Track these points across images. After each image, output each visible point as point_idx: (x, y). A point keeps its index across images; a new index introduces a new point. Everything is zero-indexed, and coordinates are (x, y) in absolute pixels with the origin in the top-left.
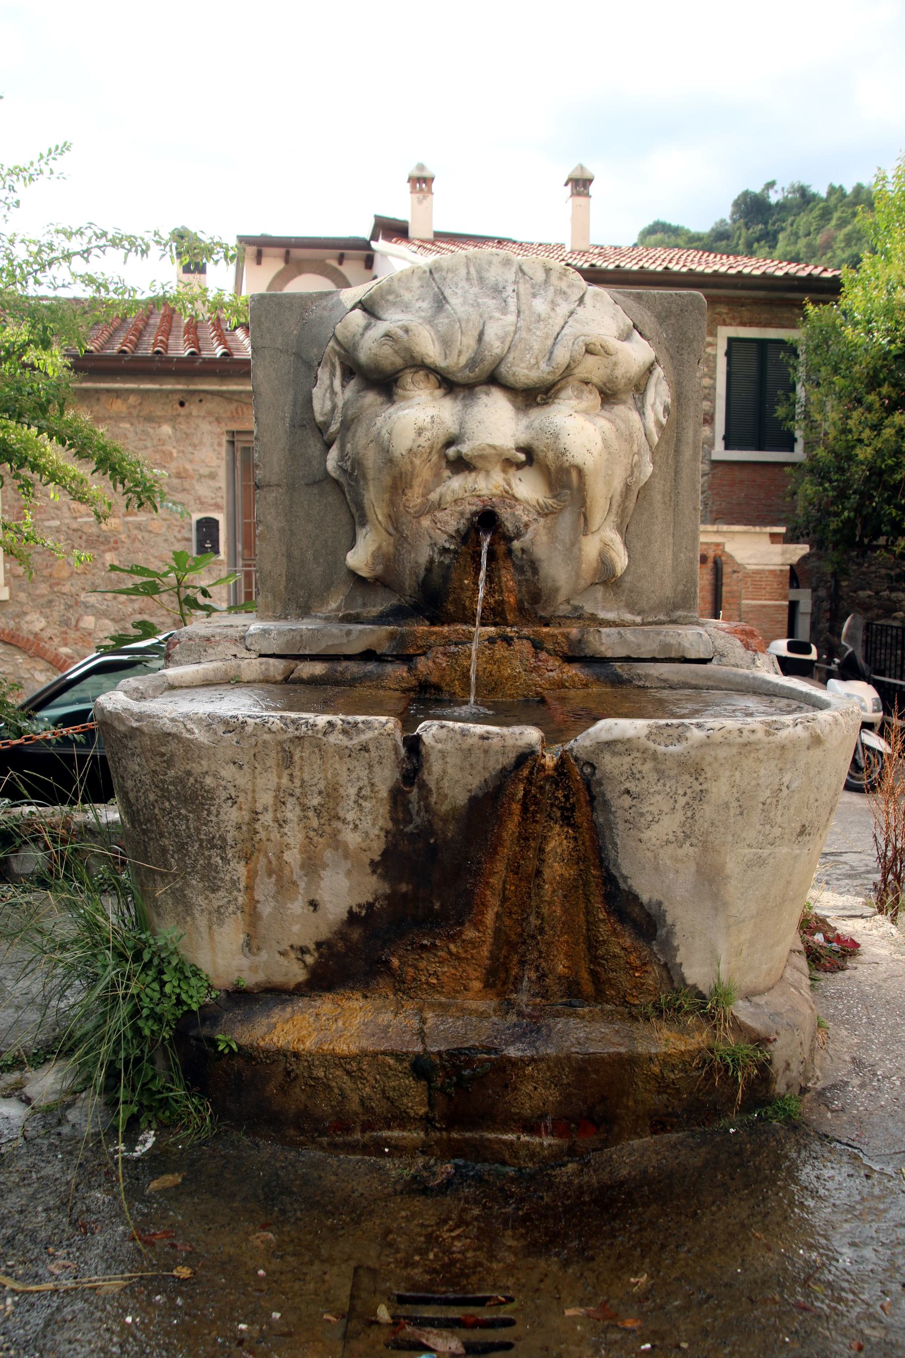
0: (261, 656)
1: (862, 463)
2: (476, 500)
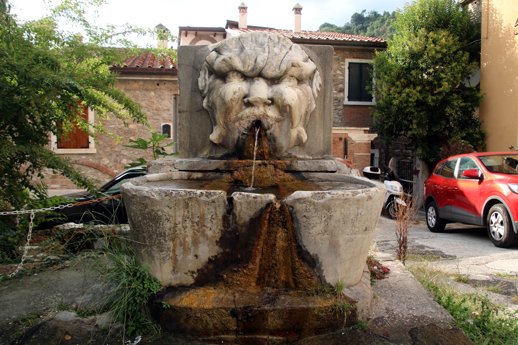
0: (180, 171)
1: (395, 105)
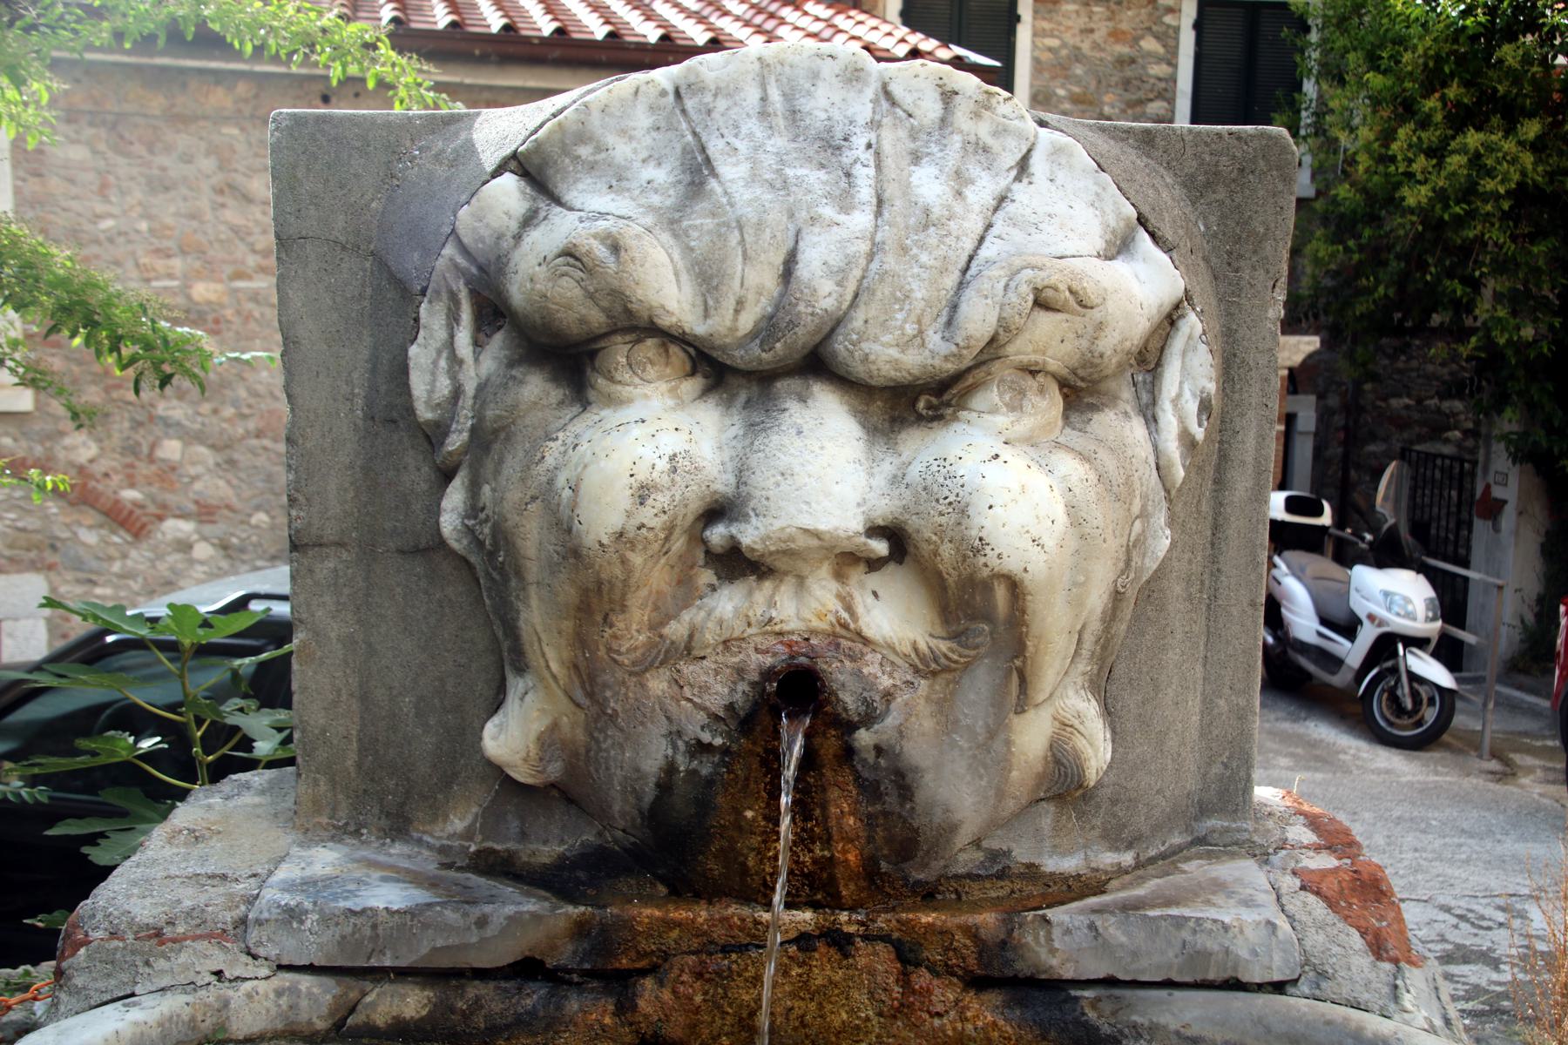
0: (280, 967)
1: (1412, 211)
2: (773, 640)
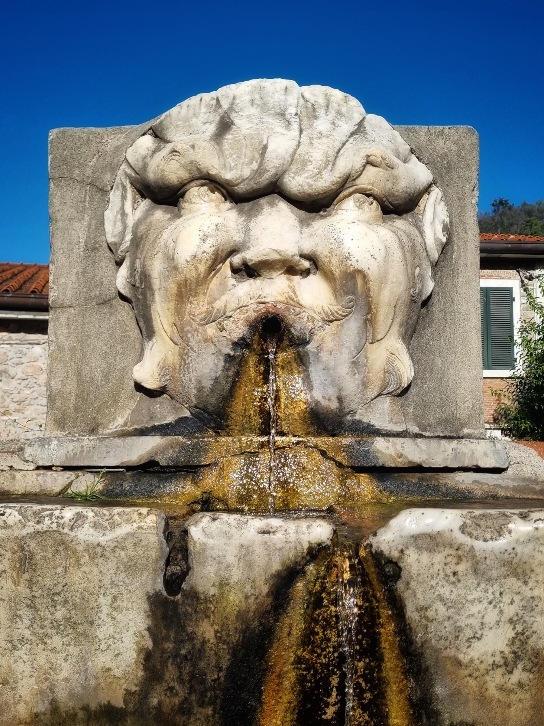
0: (38, 468)
